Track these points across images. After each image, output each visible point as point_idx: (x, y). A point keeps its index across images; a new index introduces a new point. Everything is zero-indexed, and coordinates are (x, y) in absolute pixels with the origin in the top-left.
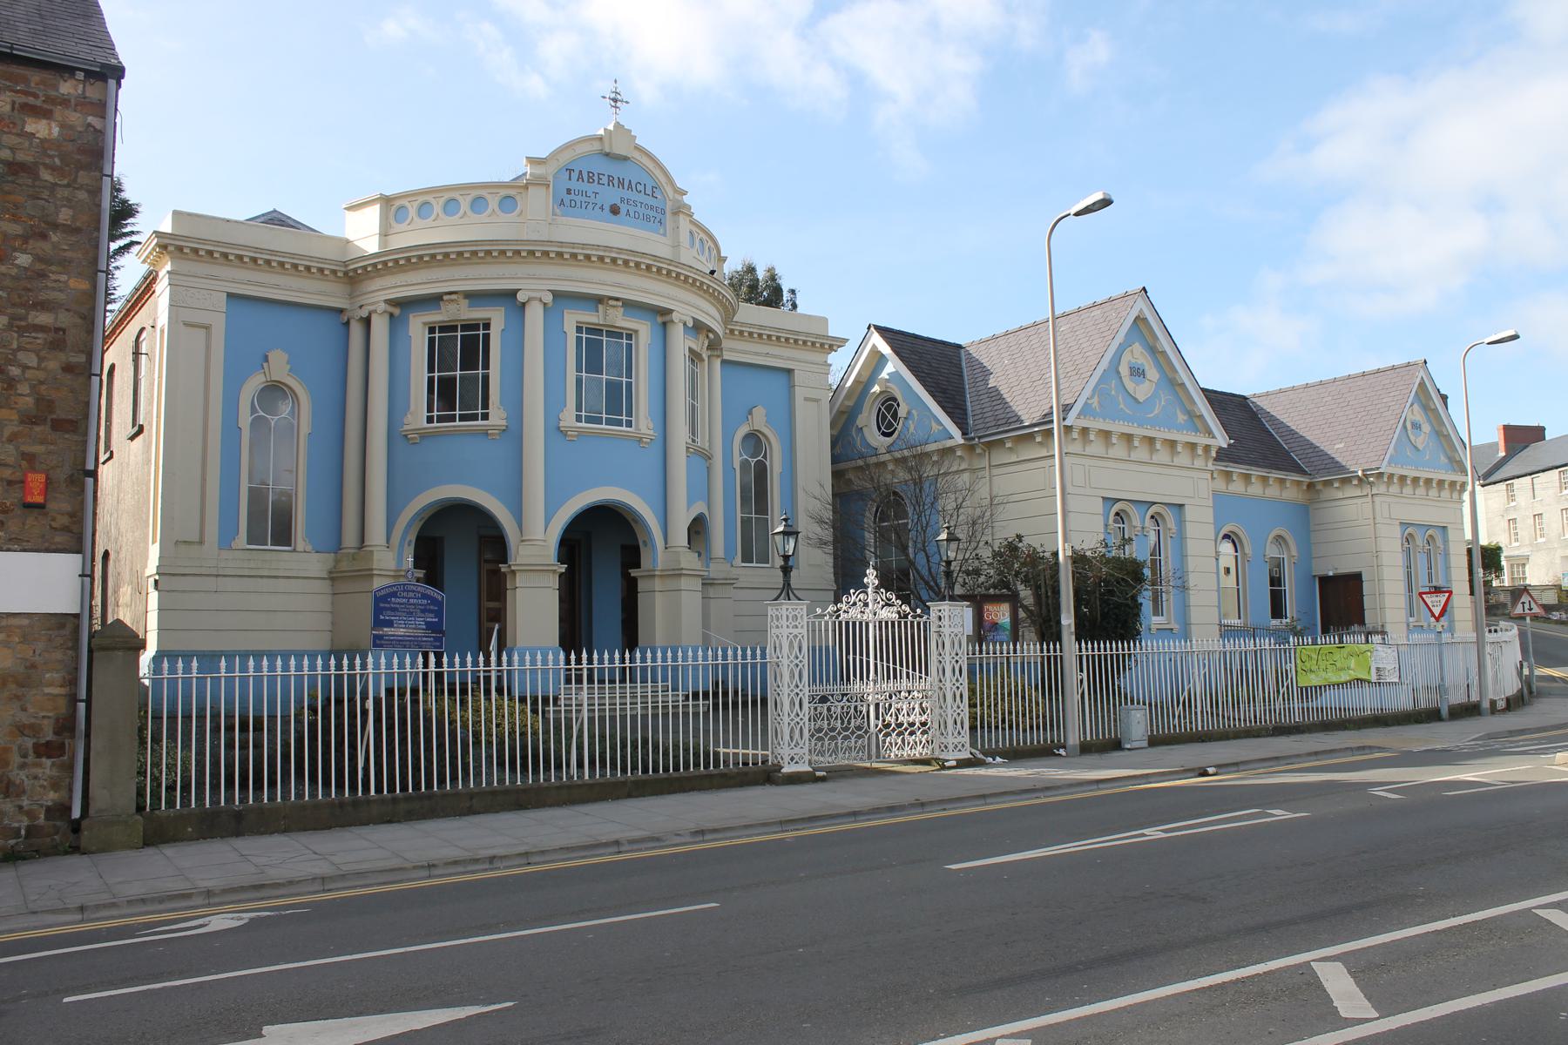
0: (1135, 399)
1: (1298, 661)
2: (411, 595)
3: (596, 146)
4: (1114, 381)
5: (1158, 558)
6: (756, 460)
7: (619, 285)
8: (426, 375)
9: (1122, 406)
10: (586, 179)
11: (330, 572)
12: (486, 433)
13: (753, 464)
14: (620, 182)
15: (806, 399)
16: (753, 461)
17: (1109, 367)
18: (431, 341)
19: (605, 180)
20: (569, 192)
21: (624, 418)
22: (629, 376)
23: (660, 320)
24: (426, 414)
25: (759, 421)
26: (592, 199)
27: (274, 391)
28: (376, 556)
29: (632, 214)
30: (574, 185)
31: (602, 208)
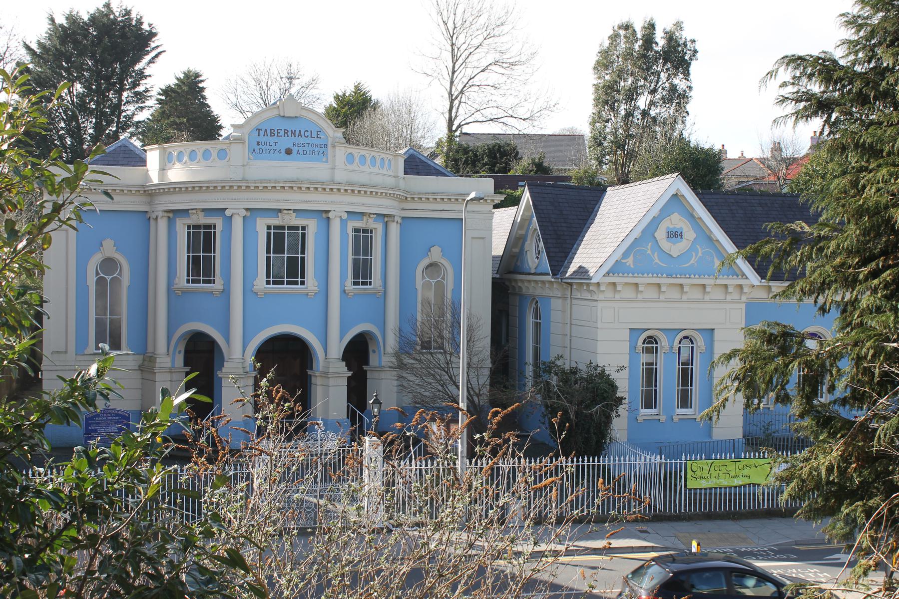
1: (689, 470)
2: (108, 415)
3: (275, 112)
5: (690, 367)
7: (288, 201)
8: (186, 255)
9: (657, 261)
10: (269, 134)
11: (139, 366)
12: (212, 293)
14: (293, 133)
15: (473, 238)
16: (433, 282)
18: (189, 233)
19: (282, 133)
20: (258, 143)
21: (299, 280)
22: (303, 252)
23: (324, 216)
24: (186, 278)
25: (436, 255)
26: (273, 147)
27: (109, 264)
28: (158, 360)
29: (301, 152)
30: (262, 139)
31: (280, 152)
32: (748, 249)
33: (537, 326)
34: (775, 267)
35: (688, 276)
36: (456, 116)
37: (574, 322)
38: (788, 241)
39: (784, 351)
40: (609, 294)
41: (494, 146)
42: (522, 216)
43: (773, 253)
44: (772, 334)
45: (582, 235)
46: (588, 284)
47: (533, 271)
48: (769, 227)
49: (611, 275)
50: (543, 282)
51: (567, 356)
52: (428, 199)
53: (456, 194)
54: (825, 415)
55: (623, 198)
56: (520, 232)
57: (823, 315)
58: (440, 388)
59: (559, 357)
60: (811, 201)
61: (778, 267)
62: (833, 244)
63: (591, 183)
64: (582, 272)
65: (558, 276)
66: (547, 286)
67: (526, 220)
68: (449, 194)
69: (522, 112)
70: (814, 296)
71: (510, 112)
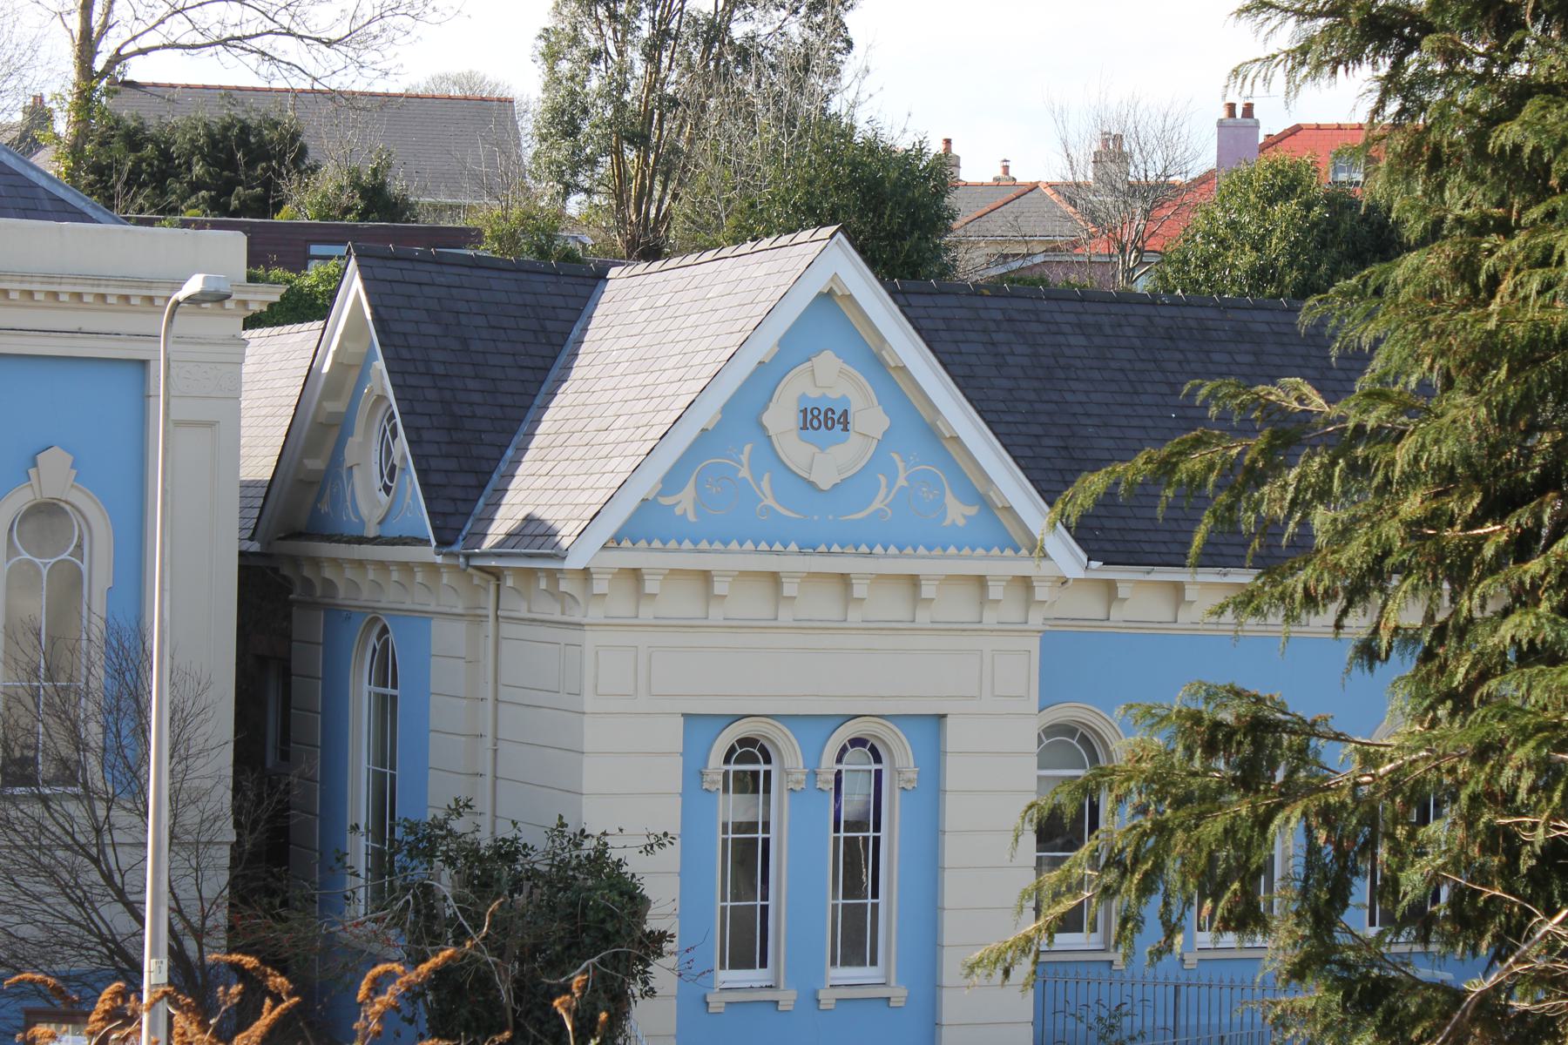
0: (812, 484)
4: (747, 448)
6: (53, 561)
9: (770, 501)
13: (45, 572)
16: (45, 564)
17: (719, 424)
32: (1140, 460)
33: (386, 708)
34: (1218, 519)
35: (864, 549)
36: (106, 27)
37: (504, 694)
38: (1260, 441)
39: (1249, 778)
40: (621, 606)
41: (227, 128)
42: (336, 353)
43: (1212, 478)
44: (1217, 725)
45: (530, 416)
46: (553, 574)
47: (371, 532)
48: (1204, 391)
49: (626, 543)
50: (407, 567)
51: (483, 803)
52: (31, 293)
53: (123, 280)
54: (1366, 976)
55: (660, 303)
56: (332, 406)
57: (1371, 668)
58: (72, 911)
59: (461, 807)
60: (1333, 322)
61: (1227, 518)
62: (1402, 454)
63: (543, 253)
64: (534, 533)
65: (456, 548)
66: (419, 577)
67: (349, 370)
68: (97, 279)
69: (323, 20)
70: (1334, 608)
71: (283, 18)
